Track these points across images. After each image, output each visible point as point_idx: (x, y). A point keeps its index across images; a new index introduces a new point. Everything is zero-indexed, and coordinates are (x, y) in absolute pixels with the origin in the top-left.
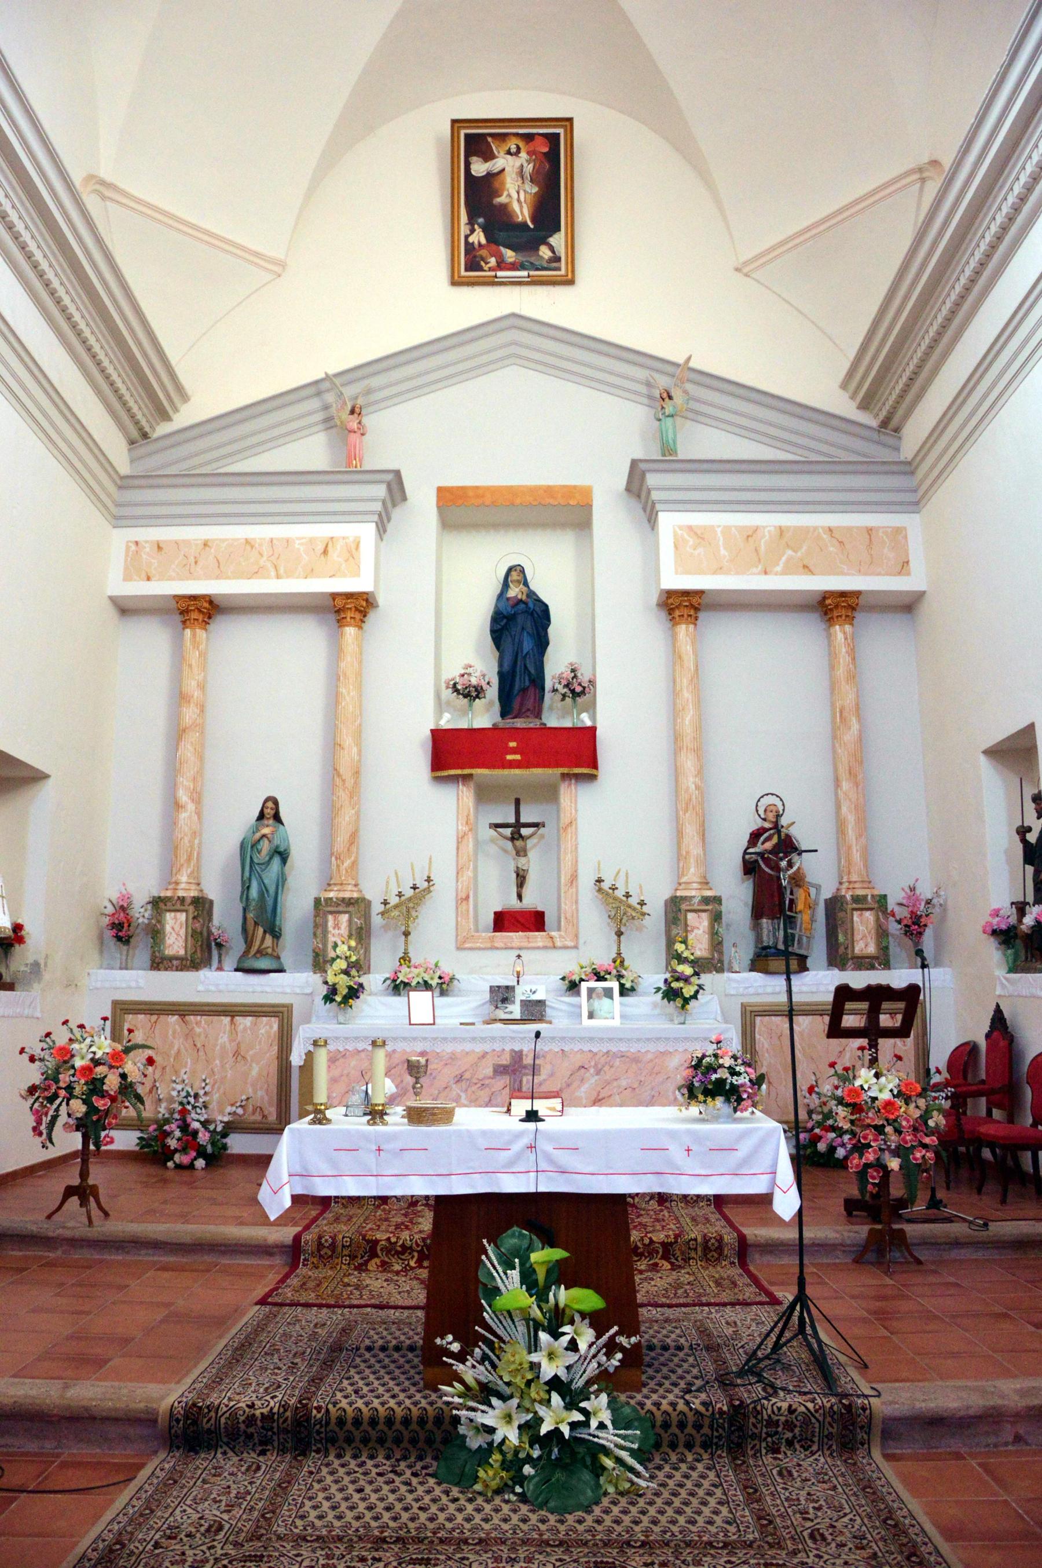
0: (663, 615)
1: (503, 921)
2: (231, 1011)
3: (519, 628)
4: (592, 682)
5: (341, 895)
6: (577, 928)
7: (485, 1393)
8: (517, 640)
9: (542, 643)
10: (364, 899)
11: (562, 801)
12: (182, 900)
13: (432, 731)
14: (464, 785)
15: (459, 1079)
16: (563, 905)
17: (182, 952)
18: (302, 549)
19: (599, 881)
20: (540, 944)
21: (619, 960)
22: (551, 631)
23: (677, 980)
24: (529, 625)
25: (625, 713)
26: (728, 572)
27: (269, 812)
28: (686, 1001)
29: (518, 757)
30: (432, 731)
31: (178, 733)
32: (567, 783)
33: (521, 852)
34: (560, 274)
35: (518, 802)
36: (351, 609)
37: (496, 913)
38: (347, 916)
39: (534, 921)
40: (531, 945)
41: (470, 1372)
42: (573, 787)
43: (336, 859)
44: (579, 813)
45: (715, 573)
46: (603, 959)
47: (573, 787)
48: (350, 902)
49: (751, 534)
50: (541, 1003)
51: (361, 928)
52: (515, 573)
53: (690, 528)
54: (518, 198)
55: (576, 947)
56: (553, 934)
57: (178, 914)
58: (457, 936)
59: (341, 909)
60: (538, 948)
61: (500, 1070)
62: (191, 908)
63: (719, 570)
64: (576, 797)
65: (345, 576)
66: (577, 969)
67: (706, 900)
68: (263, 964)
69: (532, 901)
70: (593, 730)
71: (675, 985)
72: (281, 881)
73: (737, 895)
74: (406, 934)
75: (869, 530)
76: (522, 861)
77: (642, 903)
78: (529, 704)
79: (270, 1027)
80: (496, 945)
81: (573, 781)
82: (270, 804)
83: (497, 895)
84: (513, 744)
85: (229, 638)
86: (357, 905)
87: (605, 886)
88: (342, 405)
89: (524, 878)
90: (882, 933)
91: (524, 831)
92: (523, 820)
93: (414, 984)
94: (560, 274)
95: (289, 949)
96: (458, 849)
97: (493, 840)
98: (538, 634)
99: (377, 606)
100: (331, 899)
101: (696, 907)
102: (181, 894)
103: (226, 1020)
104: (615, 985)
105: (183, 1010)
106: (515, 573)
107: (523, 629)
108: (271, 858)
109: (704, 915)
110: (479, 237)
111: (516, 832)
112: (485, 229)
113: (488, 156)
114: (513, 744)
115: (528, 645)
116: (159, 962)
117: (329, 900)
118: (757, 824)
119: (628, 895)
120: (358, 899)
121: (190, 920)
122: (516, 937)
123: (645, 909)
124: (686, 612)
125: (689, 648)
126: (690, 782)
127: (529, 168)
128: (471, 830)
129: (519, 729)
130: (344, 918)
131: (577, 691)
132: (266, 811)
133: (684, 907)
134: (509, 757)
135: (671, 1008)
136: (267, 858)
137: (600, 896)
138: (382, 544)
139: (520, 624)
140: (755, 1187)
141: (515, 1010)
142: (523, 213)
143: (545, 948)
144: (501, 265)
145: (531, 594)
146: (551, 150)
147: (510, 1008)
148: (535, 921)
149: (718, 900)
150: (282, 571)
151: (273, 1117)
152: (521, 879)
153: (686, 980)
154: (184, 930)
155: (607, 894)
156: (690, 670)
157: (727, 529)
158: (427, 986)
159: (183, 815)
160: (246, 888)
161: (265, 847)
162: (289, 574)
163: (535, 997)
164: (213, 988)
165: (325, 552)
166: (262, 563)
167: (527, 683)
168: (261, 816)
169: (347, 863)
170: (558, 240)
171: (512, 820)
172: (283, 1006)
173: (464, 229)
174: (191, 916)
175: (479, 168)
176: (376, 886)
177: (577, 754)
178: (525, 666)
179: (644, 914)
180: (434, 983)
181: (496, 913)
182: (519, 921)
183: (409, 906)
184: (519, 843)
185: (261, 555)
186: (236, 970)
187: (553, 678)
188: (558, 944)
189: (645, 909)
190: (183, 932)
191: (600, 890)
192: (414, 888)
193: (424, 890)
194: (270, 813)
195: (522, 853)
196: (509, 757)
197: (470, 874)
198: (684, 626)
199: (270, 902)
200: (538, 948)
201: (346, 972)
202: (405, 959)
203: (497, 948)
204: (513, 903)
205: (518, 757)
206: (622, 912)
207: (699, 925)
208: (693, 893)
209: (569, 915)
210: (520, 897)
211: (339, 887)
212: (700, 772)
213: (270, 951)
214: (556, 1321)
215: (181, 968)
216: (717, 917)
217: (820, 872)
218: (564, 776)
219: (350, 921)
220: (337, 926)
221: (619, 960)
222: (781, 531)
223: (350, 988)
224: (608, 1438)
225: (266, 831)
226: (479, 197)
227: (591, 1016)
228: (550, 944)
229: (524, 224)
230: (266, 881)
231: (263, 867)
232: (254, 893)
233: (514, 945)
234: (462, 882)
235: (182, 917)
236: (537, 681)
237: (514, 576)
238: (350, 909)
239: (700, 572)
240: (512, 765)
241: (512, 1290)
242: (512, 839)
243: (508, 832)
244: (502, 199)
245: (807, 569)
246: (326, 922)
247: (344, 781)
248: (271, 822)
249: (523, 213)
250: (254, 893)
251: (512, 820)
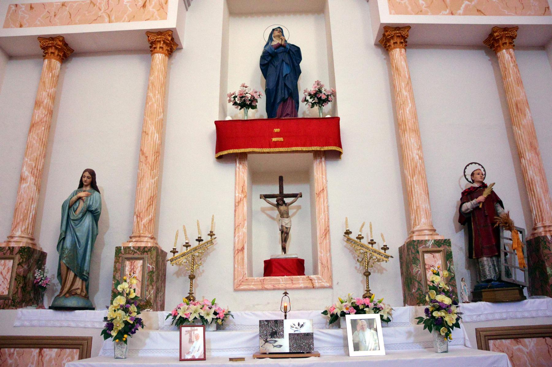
0: (379, 51)
1: (272, 268)
3: (280, 60)
4: (334, 94)
5: (139, 245)
6: (331, 271)
8: (278, 70)
9: (297, 72)
10: (157, 249)
11: (315, 173)
12: (12, 249)
13: (217, 123)
14: (240, 163)
16: (319, 254)
17: (6, 293)
18: (128, 4)
19: (348, 233)
20: (302, 285)
21: (368, 295)
22: (301, 65)
23: (439, 309)
24: (287, 59)
26: (426, 13)
27: (87, 180)
28: (449, 329)
29: (281, 139)
30: (217, 123)
32: (318, 161)
33: (284, 215)
35: (281, 179)
37: (266, 262)
38: (141, 261)
39: (296, 267)
40: (294, 286)
42: (323, 163)
43: (137, 216)
44: (328, 182)
45: (417, 14)
46: (358, 296)
47: (323, 163)
48: (144, 250)
50: (309, 336)
51: (152, 272)
55: (331, 287)
56: (312, 277)
57: (7, 261)
58: (234, 279)
59: (136, 256)
60: (301, 288)
62: (18, 257)
63: (420, 12)
64: (326, 170)
65: (156, 19)
66: (338, 304)
67: (438, 243)
68: (71, 302)
69: (293, 252)
70: (336, 120)
71: (436, 314)
72: (93, 235)
74: (192, 277)
76: (285, 221)
77: (385, 248)
78: (289, 110)
80: (266, 286)
81: (323, 159)
82: (87, 174)
83: (267, 248)
84: (277, 130)
85: (84, 75)
86: (159, 256)
87: (353, 236)
89: (287, 233)
91: (287, 200)
92: (285, 192)
93: (191, 319)
96: (235, 211)
97: (263, 210)
98: (294, 65)
99: (181, 48)
100: (129, 248)
101: (430, 248)
102: (12, 245)
103: (35, 351)
104: (377, 317)
107: (283, 61)
108: (83, 216)
109: (437, 255)
111: (280, 200)
114: (277, 130)
115: (286, 70)
117: (127, 249)
118: (465, 185)
119: (372, 243)
120: (151, 247)
121: (16, 266)
122: (282, 280)
123: (388, 252)
124: (398, 41)
125: (403, 63)
126: (413, 153)
128: (245, 197)
129: (281, 126)
130: (139, 263)
132: (84, 179)
133: (421, 249)
134: (274, 139)
135: (432, 336)
136: (80, 216)
137: (349, 245)
138: (188, 14)
139: (281, 61)
141: (284, 344)
143: (306, 288)
147: (280, 341)
148: (296, 267)
150: (113, 18)
152: (285, 234)
153: (447, 309)
154: (10, 274)
155: (355, 243)
156: (405, 77)
158: (203, 322)
159: (24, 185)
160: (62, 239)
161: (81, 206)
162: (118, 19)
163: (303, 330)
164: (27, 323)
165: (144, 6)
166: (100, 14)
167: (287, 96)
168: (81, 185)
169: (145, 220)
171: (277, 192)
172: (83, 339)
174: (17, 262)
177: (326, 138)
178: (285, 85)
179: (387, 257)
180: (209, 318)
181: (266, 262)
184: (283, 208)
185: (100, 10)
186: (50, 308)
187: (305, 91)
188: (317, 285)
189: (388, 252)
190: (8, 277)
191: (349, 239)
192: (199, 240)
193: (207, 243)
195: (285, 215)
196: (274, 139)
197: (245, 230)
198: (398, 50)
199: (81, 251)
200: (301, 288)
201: (125, 309)
202: (190, 299)
203: (267, 289)
204: (279, 254)
205: (281, 139)
206: (367, 257)
208: (427, 238)
209: (325, 262)
210: (284, 249)
211: (137, 239)
212: (420, 148)
213: (79, 291)
218: (317, 154)
219: (143, 266)
220: (133, 271)
223: (126, 323)
225: (82, 194)
227: (357, 347)
228: (311, 286)
230: (78, 234)
231: (77, 222)
232: (68, 243)
233: (280, 286)
234: (239, 237)
235: (10, 263)
236: (293, 94)
237: (276, 33)
238: (145, 256)
239: (407, 13)
240: (276, 145)
242: (278, 205)
243: (274, 201)
245: (480, 12)
246: (124, 267)
247: (146, 157)
248: (88, 188)
250: (68, 243)
251: (277, 192)
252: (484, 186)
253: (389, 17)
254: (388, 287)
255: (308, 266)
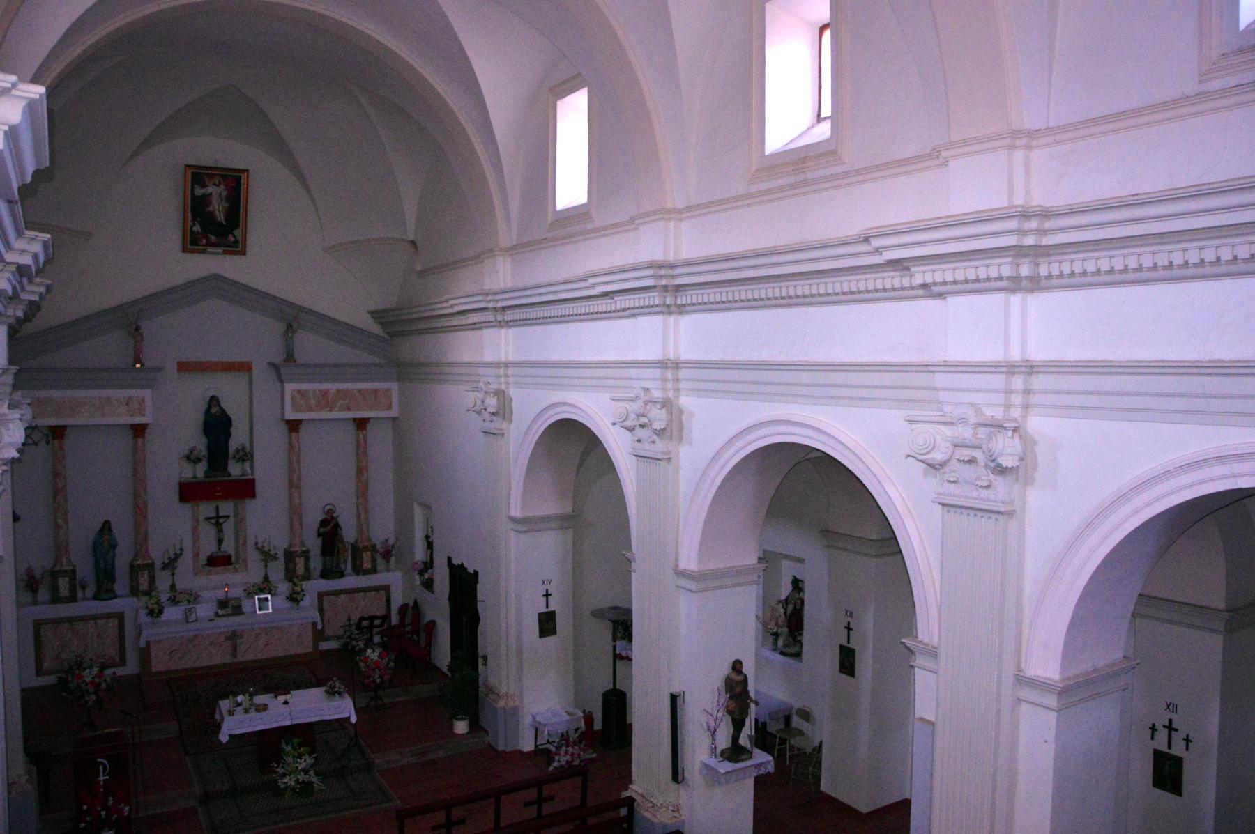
2: (95, 618)
7: (284, 775)
9: (228, 435)
15: (211, 644)
22: (233, 429)
25: (267, 468)
31: (57, 491)
34: (237, 248)
36: (139, 430)
41: (281, 771)
49: (325, 393)
52: (214, 400)
53: (299, 391)
54: (218, 209)
61: (227, 638)
67: (303, 552)
73: (314, 544)
75: (376, 391)
79: (114, 623)
83: (208, 546)
88: (130, 319)
90: (374, 561)
94: (237, 248)
95: (121, 586)
105: (71, 620)
106: (214, 400)
110: (197, 228)
111: (217, 522)
112: (201, 224)
113: (204, 186)
116: (55, 599)
127: (224, 193)
129: (218, 476)
131: (245, 456)
139: (217, 424)
140: (346, 715)
142: (220, 216)
144: (209, 244)
145: (223, 411)
146: (234, 181)
149: (308, 551)
151: (117, 659)
152: (220, 542)
157: (314, 392)
160: (97, 563)
170: (238, 232)
171: (213, 515)
173: (189, 223)
175: (199, 191)
176: (157, 550)
177: (245, 489)
182: (218, 561)
183: (171, 564)
194: (106, 527)
207: (300, 563)
214: (300, 756)
215: (69, 602)
216: (307, 559)
217: (349, 533)
221: (266, 578)
222: (338, 391)
224: (315, 779)
226: (197, 207)
229: (220, 224)
235: (67, 579)
241: (289, 748)
244: (211, 209)
245: (349, 409)
249: (220, 216)
251: (213, 515)
252: (333, 518)
253: (290, 415)
254: (277, 571)
255: (233, 559)
